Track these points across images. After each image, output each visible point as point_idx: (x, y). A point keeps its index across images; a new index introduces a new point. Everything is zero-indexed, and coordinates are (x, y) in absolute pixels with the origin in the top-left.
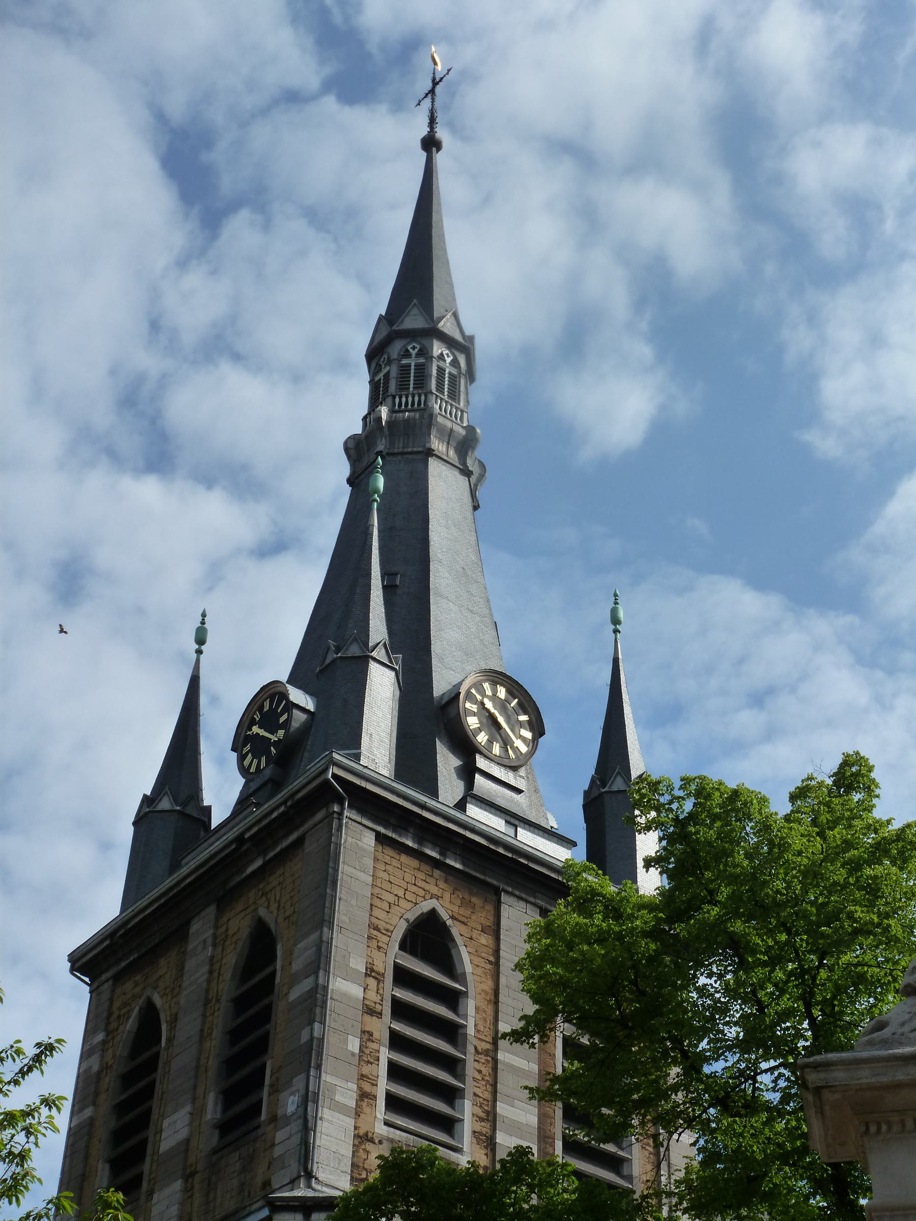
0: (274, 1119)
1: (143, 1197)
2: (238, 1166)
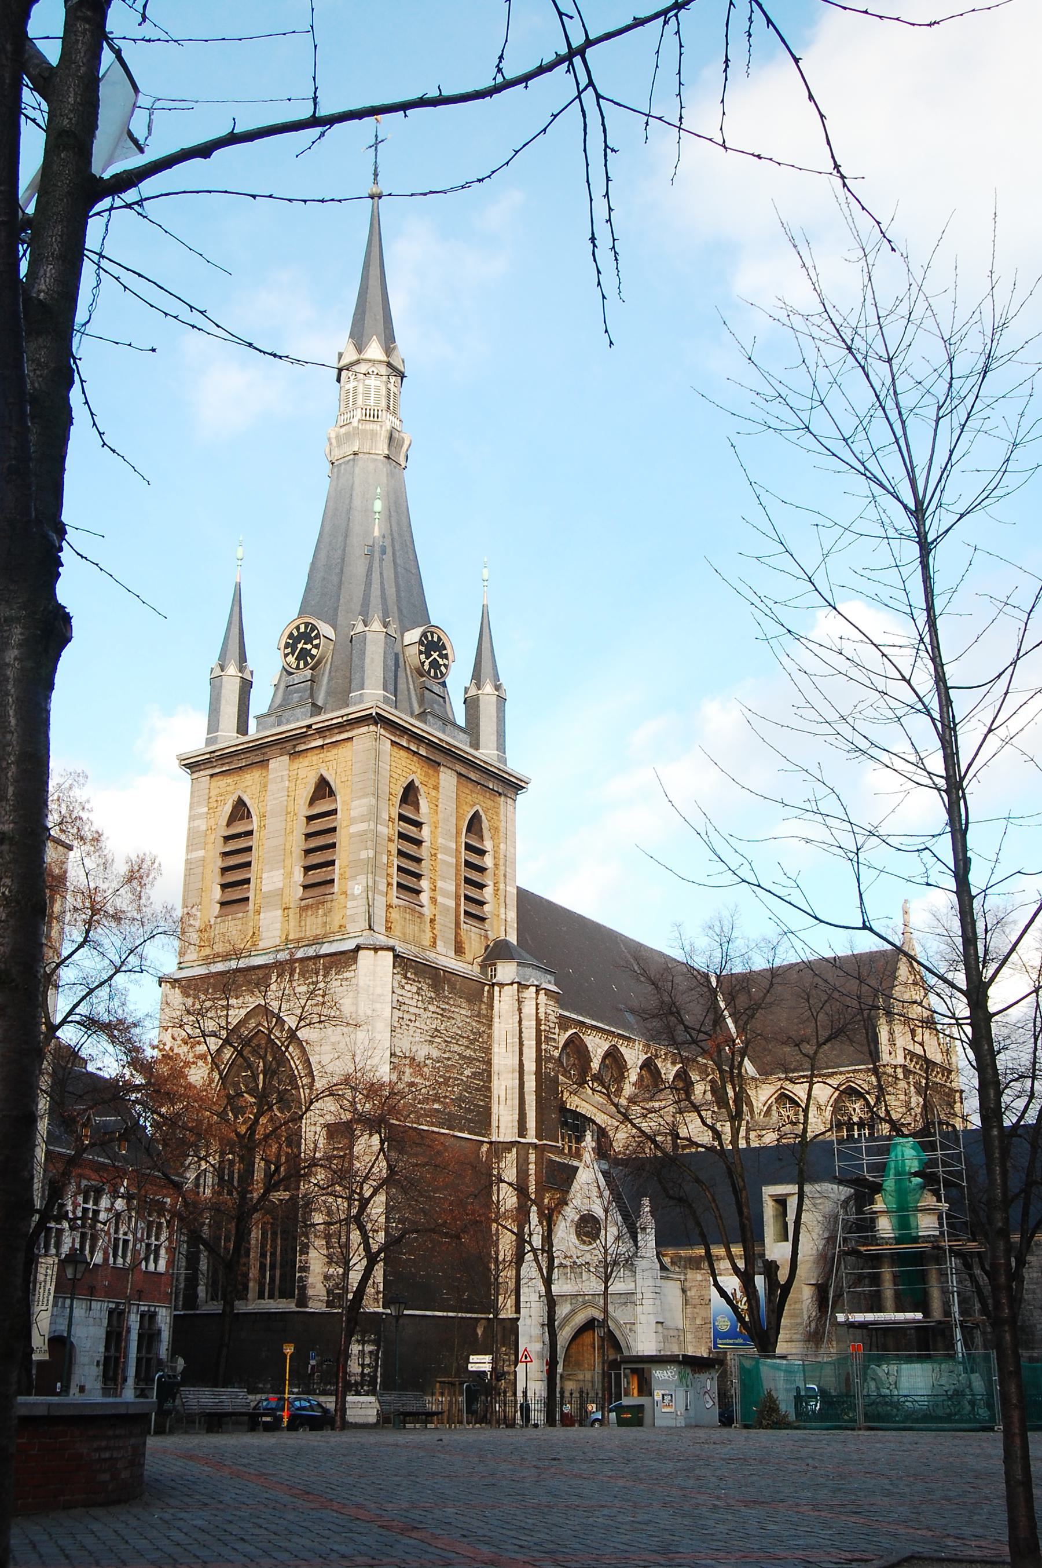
0: (345, 893)
1: (251, 913)
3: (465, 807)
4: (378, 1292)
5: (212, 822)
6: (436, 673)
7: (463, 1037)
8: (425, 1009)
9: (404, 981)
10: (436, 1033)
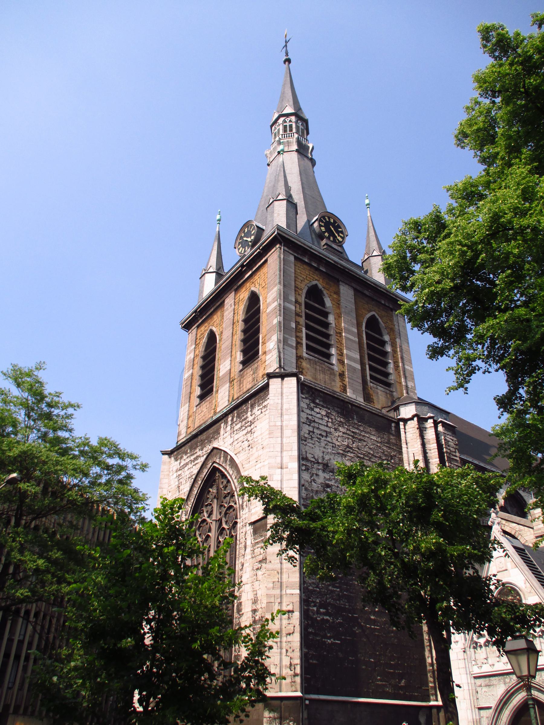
2: (251, 373)
3: (363, 311)
4: (296, 675)
5: (197, 352)
6: (325, 219)
7: (376, 457)
8: (336, 429)
9: (312, 405)
10: (348, 449)
